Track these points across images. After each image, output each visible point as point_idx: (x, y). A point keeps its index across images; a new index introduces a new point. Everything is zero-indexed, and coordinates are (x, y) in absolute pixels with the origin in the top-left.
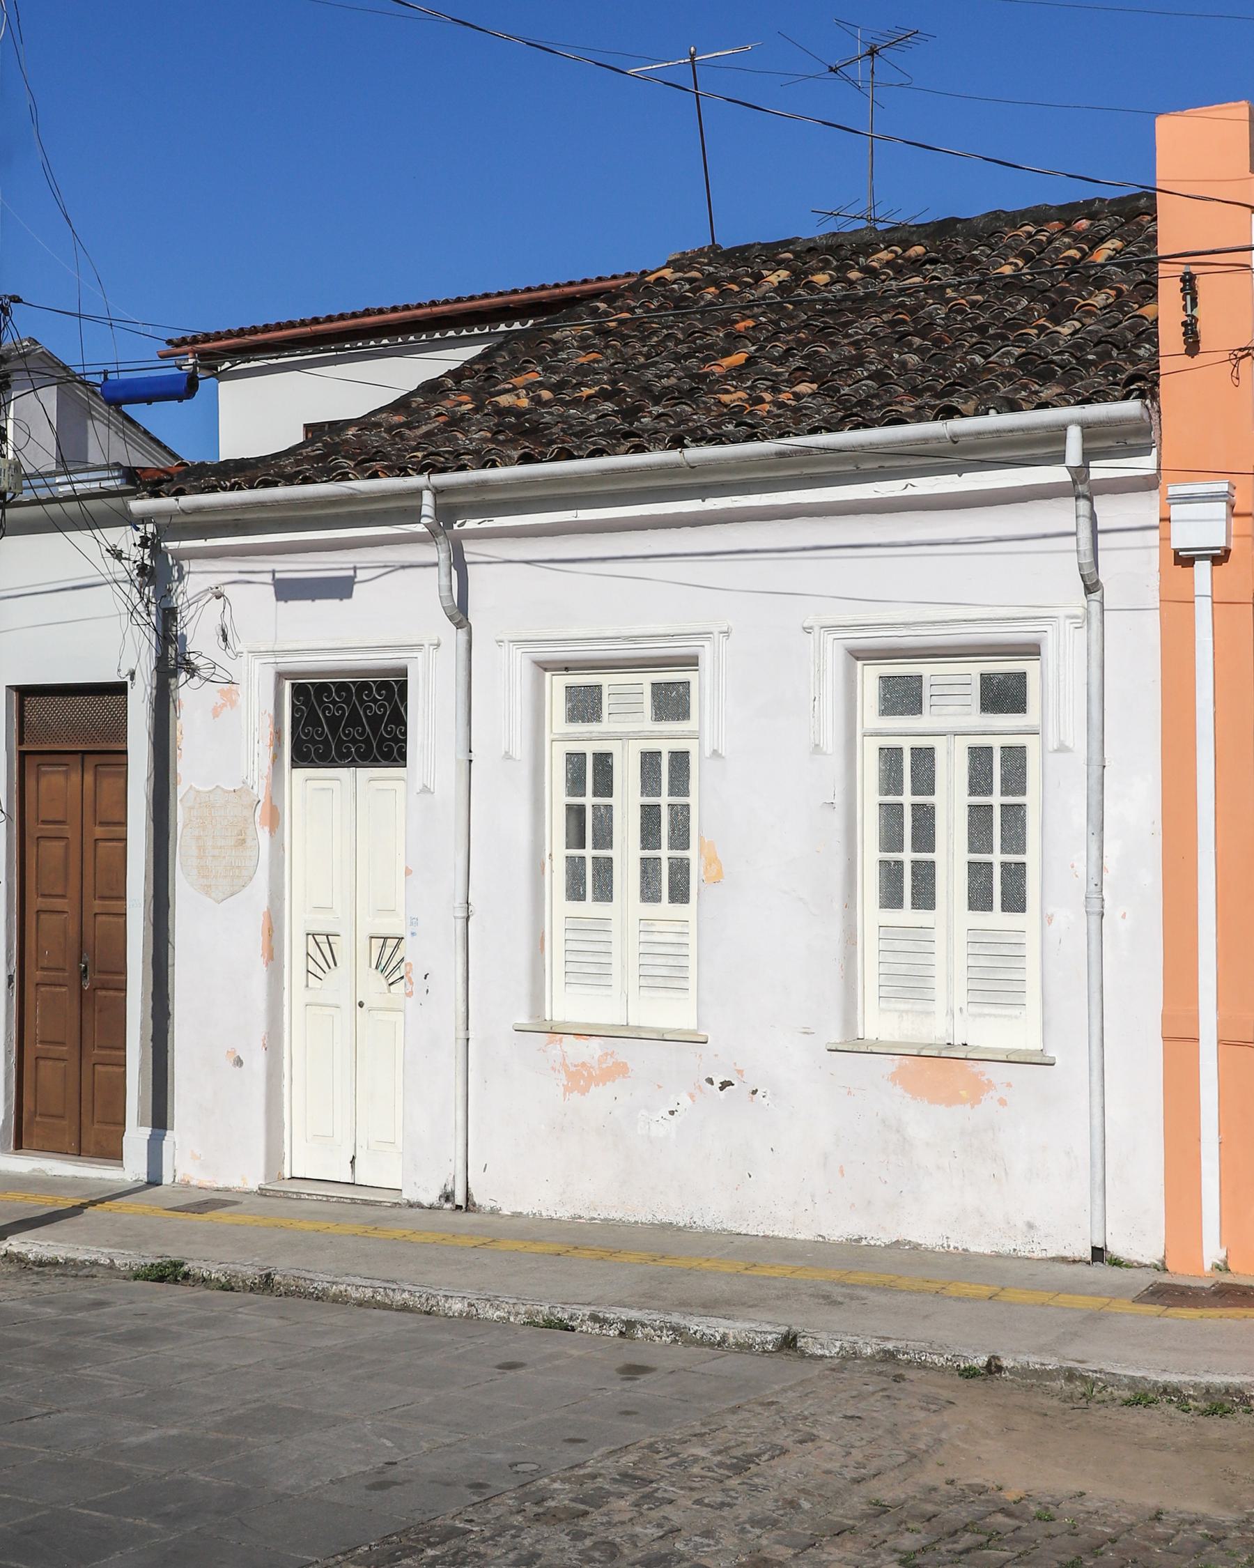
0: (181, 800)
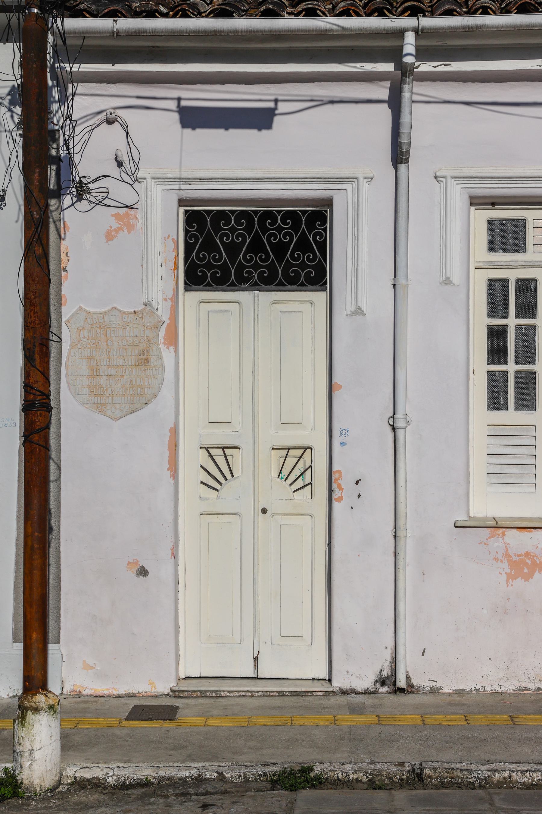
0: (68, 321)
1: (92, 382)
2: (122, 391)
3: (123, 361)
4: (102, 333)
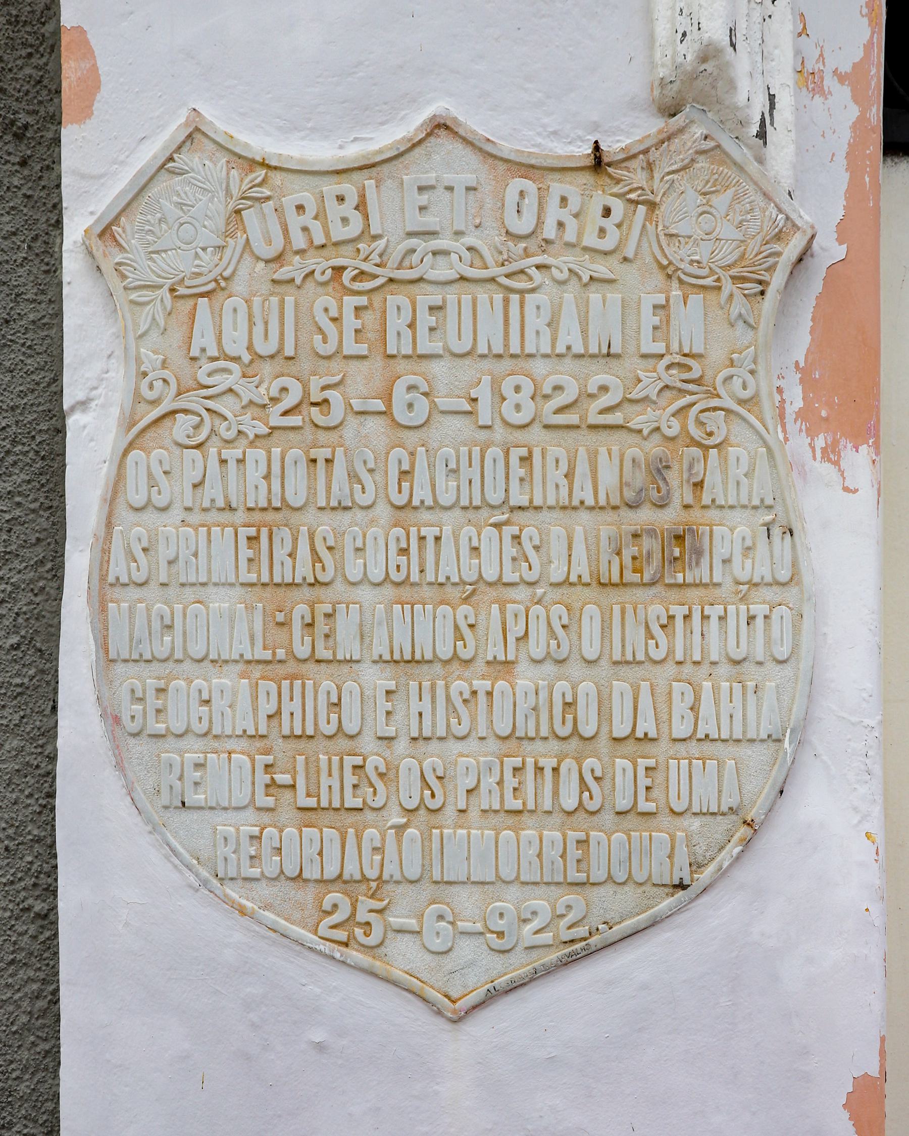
1: (279, 712)
2: (500, 783)
3: (510, 551)
4: (350, 322)
